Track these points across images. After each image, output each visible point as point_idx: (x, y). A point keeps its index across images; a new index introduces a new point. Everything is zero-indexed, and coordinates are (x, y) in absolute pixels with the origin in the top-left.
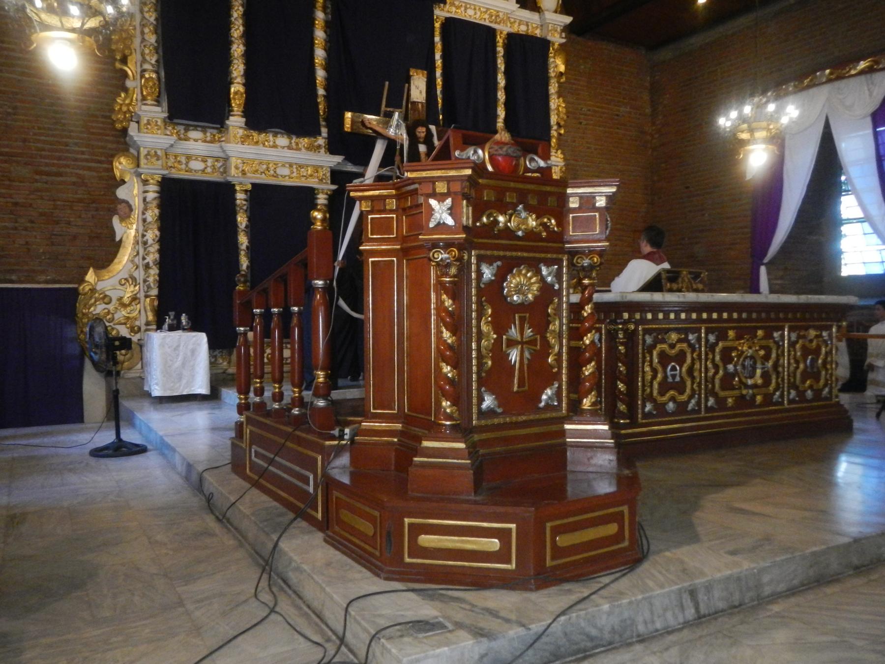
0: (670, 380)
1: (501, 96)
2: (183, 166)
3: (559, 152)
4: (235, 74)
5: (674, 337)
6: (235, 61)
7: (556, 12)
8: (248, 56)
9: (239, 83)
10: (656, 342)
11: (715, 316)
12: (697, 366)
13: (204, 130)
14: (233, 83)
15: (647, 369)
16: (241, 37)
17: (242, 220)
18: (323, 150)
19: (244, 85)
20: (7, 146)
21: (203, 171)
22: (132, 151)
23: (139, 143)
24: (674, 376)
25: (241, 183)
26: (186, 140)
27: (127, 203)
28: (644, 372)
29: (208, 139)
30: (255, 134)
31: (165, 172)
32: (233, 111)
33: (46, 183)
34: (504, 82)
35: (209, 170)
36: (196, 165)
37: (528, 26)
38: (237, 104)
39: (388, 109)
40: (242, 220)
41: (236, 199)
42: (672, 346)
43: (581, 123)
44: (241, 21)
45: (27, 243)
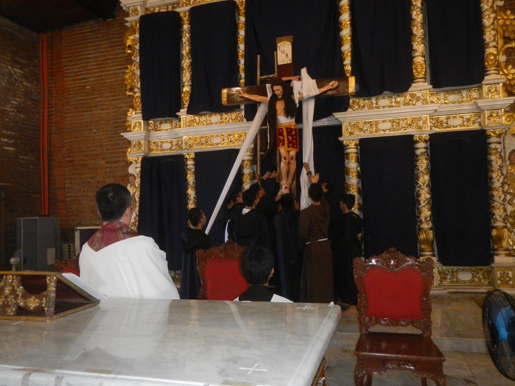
1: (418, 31)
2: (159, 148)
3: (510, 67)
4: (184, 79)
6: (184, 71)
8: (193, 66)
9: (187, 85)
13: (171, 122)
14: (184, 86)
16: (188, 54)
17: (191, 178)
18: (245, 119)
19: (190, 85)
20: (94, 150)
21: (171, 149)
25: (188, 154)
26: (160, 131)
27: (133, 175)
29: (174, 127)
30: (196, 118)
31: (143, 154)
32: (184, 105)
33: (111, 168)
34: (421, 16)
35: (174, 147)
36: (166, 146)
38: (186, 100)
39: (263, 77)
40: (191, 178)
41: (187, 165)
44: (187, 43)
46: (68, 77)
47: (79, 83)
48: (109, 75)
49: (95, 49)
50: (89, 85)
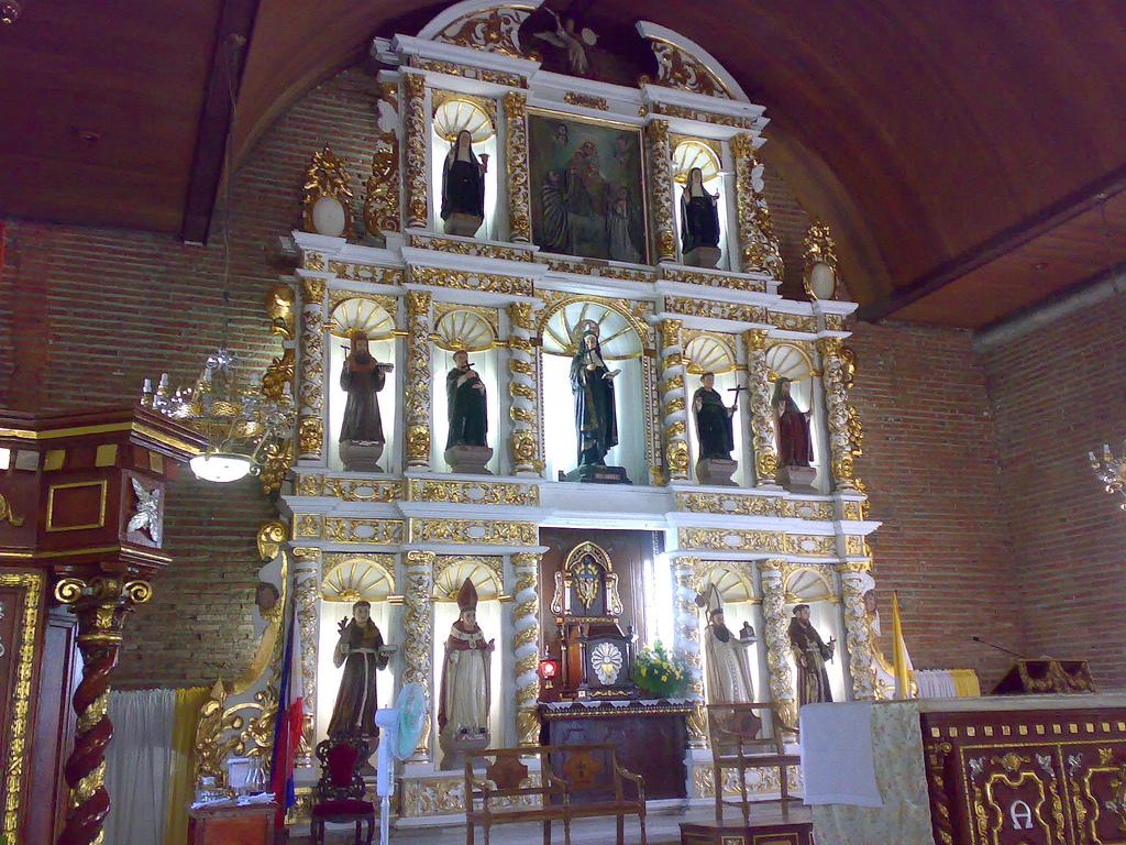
0: (1017, 826)
5: (1015, 760)
7: (832, 298)
10: (988, 769)
11: (1023, 730)
12: (1058, 805)
15: (979, 809)
22: (282, 518)
23: (292, 508)
24: (1022, 821)
27: (271, 586)
28: (974, 814)
37: (796, 320)
42: (1014, 776)
43: (887, 438)
45: (139, 648)
46: (58, 338)
47: (92, 360)
48: (180, 358)
49: (147, 295)
50: (122, 370)
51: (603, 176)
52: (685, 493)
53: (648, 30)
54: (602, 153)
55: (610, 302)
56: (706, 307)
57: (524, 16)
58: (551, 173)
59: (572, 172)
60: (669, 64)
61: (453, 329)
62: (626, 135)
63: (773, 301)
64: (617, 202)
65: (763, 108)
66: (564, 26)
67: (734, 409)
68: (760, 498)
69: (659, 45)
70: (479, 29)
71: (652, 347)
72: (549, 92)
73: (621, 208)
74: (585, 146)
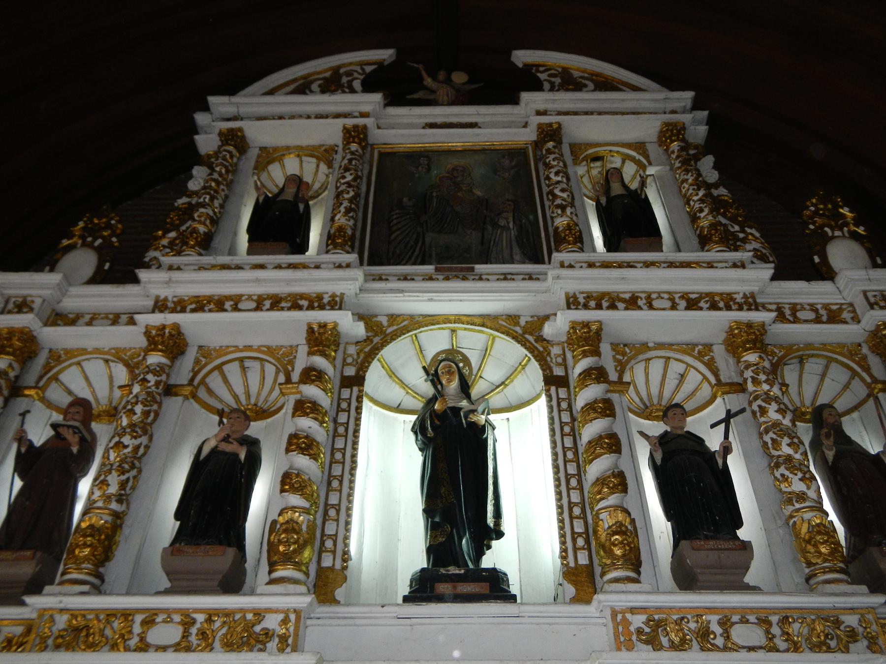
51: (478, 193)
52: (633, 610)
53: (522, 57)
54: (479, 172)
55: (487, 321)
56: (640, 303)
57: (369, 69)
58: (405, 200)
59: (435, 194)
60: (558, 80)
61: (247, 387)
62: (517, 154)
63: (756, 277)
64: (499, 214)
65: (689, 95)
66: (434, 77)
67: (726, 449)
68: (823, 615)
69: (541, 69)
70: (315, 87)
71: (558, 372)
72: (407, 128)
73: (508, 221)
74: (454, 169)
